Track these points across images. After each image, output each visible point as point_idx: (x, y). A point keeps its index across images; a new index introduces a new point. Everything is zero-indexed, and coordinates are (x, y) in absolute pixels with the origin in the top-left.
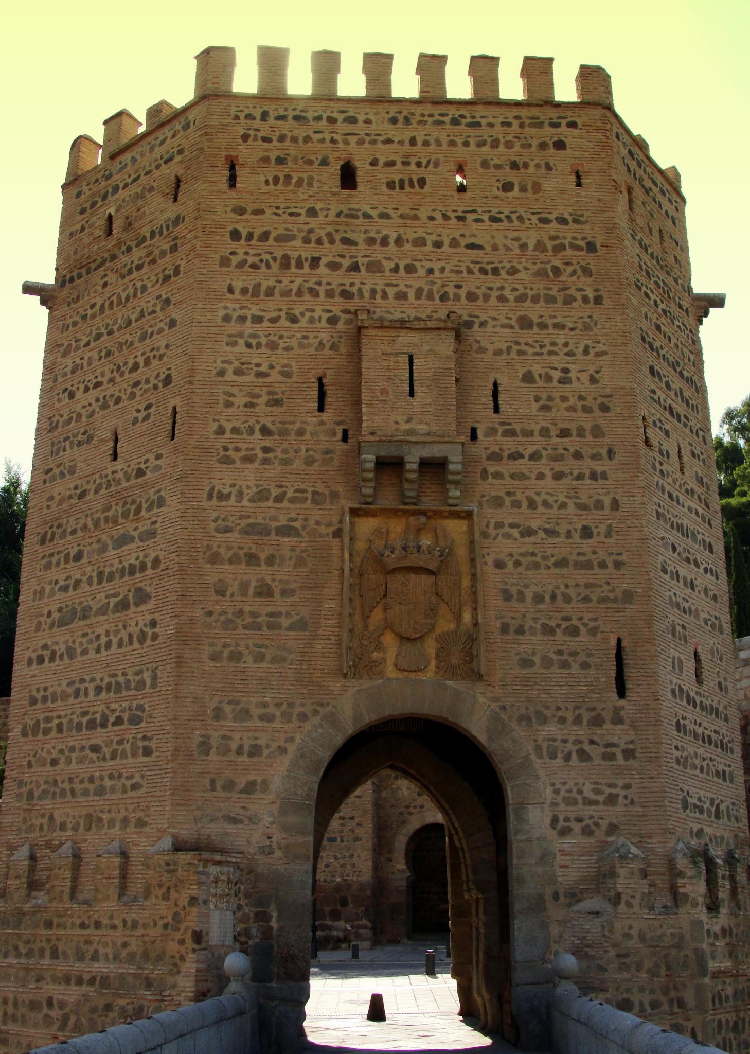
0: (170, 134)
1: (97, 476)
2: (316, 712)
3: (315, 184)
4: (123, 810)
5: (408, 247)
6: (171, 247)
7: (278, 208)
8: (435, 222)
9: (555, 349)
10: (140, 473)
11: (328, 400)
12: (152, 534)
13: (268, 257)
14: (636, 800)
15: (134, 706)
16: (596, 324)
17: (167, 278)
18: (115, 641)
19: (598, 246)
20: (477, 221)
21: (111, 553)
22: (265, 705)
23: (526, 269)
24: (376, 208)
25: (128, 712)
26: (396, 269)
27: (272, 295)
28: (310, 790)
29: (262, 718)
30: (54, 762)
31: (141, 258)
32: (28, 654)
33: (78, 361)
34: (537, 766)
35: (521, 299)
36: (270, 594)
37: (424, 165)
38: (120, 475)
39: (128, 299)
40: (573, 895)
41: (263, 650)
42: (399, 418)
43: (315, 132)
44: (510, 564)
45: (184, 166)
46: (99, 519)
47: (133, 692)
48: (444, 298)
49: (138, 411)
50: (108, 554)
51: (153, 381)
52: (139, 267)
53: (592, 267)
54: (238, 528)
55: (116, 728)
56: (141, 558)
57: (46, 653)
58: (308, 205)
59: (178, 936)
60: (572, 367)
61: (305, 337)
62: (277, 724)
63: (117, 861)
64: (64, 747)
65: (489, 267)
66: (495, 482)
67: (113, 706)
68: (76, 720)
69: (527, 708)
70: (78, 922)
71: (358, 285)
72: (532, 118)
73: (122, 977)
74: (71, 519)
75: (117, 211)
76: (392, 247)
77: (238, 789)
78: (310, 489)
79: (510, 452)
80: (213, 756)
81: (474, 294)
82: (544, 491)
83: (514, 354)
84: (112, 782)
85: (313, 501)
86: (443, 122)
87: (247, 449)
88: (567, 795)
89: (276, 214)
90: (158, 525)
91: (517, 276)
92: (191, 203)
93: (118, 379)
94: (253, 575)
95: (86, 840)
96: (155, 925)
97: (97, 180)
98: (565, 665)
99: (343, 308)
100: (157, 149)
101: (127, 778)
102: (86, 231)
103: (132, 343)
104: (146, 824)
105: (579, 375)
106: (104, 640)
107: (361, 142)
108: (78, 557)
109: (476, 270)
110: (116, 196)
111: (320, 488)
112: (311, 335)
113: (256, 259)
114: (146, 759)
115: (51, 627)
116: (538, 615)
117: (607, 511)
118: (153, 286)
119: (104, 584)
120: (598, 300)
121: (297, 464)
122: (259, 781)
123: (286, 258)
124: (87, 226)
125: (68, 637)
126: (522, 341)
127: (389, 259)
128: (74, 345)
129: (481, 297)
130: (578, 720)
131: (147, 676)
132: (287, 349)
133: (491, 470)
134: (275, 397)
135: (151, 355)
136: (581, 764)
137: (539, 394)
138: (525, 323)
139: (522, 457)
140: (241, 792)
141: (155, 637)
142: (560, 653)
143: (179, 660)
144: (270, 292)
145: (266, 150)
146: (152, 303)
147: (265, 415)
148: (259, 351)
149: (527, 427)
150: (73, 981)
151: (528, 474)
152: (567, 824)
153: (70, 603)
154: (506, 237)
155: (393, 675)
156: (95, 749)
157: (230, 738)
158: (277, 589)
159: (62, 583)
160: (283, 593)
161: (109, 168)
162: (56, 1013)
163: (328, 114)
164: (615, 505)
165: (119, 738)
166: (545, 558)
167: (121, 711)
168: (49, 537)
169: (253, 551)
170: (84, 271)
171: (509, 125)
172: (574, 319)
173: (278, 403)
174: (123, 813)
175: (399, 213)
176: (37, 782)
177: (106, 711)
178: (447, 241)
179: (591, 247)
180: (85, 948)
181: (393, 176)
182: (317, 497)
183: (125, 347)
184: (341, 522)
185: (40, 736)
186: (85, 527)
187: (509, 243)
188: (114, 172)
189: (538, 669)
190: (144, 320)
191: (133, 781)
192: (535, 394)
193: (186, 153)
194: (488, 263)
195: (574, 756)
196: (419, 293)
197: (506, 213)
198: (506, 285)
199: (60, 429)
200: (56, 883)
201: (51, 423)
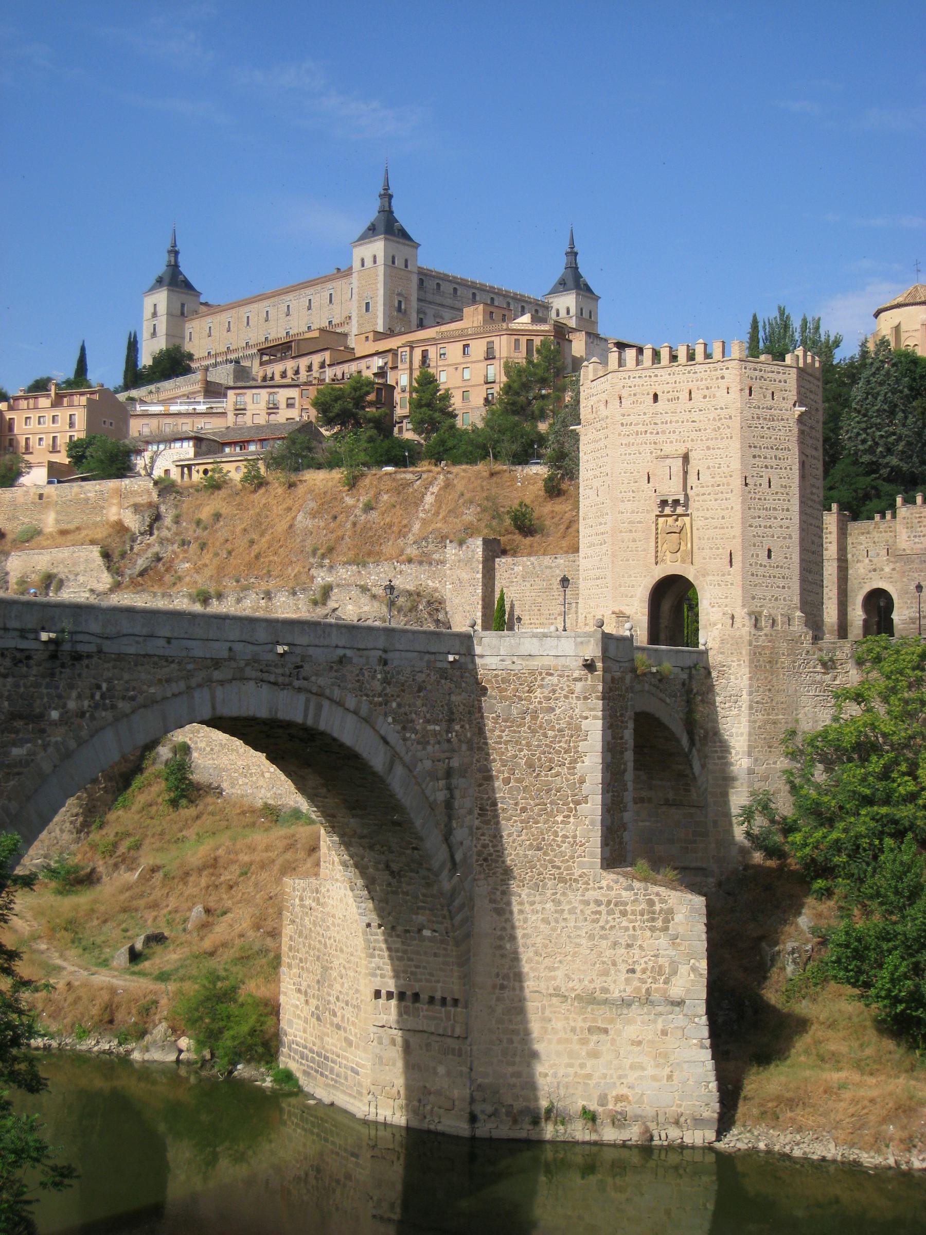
121: (642, 501)
138: (708, 448)
147: (634, 486)
164: (732, 508)
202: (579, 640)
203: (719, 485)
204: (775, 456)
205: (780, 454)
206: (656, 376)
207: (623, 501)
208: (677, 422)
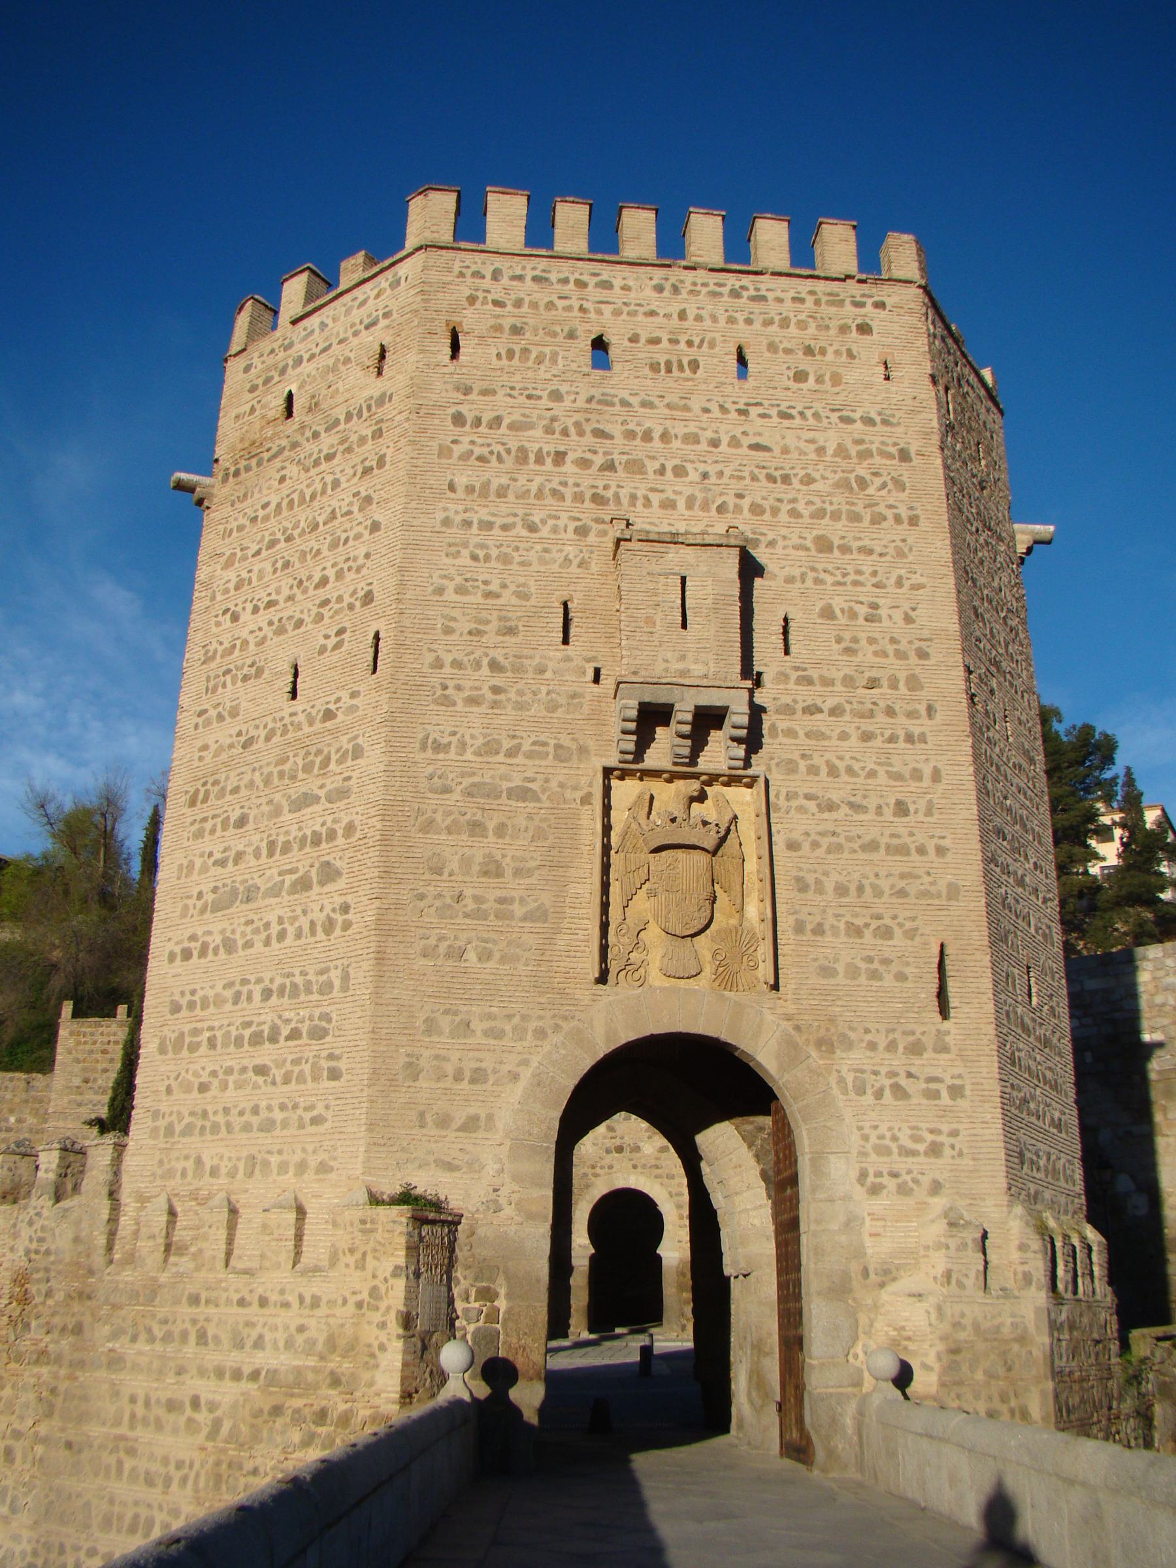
0: (373, 294)
1: (269, 719)
2: (557, 1028)
3: (560, 361)
4: (299, 1151)
5: (676, 444)
6: (374, 433)
7: (512, 388)
8: (711, 415)
9: (861, 578)
10: (329, 715)
11: (573, 631)
12: (342, 794)
13: (500, 448)
14: (965, 1151)
15: (317, 1015)
16: (911, 549)
17: (367, 471)
18: (291, 930)
19: (913, 455)
20: (763, 416)
21: (287, 817)
22: (490, 1017)
23: (823, 478)
24: (636, 394)
25: (307, 1022)
26: (662, 471)
27: (505, 496)
28: (549, 1128)
29: (487, 1033)
30: (203, 1088)
31: (332, 446)
32: (170, 946)
33: (245, 575)
34: (841, 1104)
35: (819, 514)
36: (499, 873)
37: (696, 344)
38: (301, 718)
39: (313, 497)
40: (887, 1272)
41: (490, 945)
42: (669, 655)
43: (560, 298)
44: (806, 846)
45: (391, 332)
46: (270, 774)
47: (316, 997)
48: (721, 509)
49: (327, 637)
50: (282, 819)
51: (347, 599)
52: (330, 457)
53: (904, 479)
54: (459, 788)
55: (290, 1043)
56: (329, 824)
57: (195, 946)
58: (551, 388)
59: (377, 1317)
60: (881, 602)
61: (546, 551)
62: (506, 1042)
63: (292, 1216)
64: (217, 1068)
65: (777, 474)
66: (785, 740)
67: (287, 1015)
68: (234, 1033)
69: (828, 1030)
70: (236, 1297)
71: (613, 489)
72: (830, 294)
73: (298, 1371)
74: (232, 774)
75: (300, 388)
76: (657, 443)
77: (455, 1125)
78: (552, 742)
79: (806, 704)
80: (423, 1083)
81: (760, 506)
82: (847, 756)
83: (809, 583)
84: (284, 1114)
85: (557, 757)
86: (720, 294)
87: (471, 688)
88: (878, 1142)
89: (510, 395)
90: (351, 782)
91: (813, 487)
92: (400, 377)
93: (299, 596)
94: (479, 849)
95: (246, 1191)
96: (345, 1301)
97: (272, 351)
98: (874, 975)
99: (594, 516)
100: (355, 311)
101: (306, 1109)
102: (257, 413)
103: (319, 552)
104: (332, 1169)
105: (890, 612)
106: (275, 929)
107: (617, 313)
108: (242, 822)
109: (762, 477)
110: (299, 370)
111: (565, 741)
112: (554, 548)
113: (485, 451)
114: (333, 1084)
115: (203, 911)
116: (842, 911)
117: (926, 782)
118: (348, 481)
119: (277, 856)
120: (913, 521)
122: (483, 1116)
123: (522, 450)
124: (258, 407)
125: (225, 924)
126: (820, 566)
127: (653, 458)
128: (239, 554)
129: (768, 510)
130: (891, 1046)
131: (335, 976)
132: (522, 564)
133: (782, 725)
134: (508, 624)
135: (346, 567)
136: (896, 1103)
137: (841, 633)
138: (824, 545)
139: (820, 711)
140: (458, 1130)
141: (347, 926)
142: (870, 960)
143: (380, 956)
144: (502, 492)
145: (498, 317)
146: (347, 501)
147: (495, 645)
148: (487, 565)
149: (826, 674)
150: (227, 1375)
151: (828, 733)
152: (879, 1180)
153: (229, 881)
154: (799, 438)
155: (657, 984)
156: (261, 1070)
157: (446, 1059)
158: (508, 865)
159: (218, 856)
160: (517, 873)
161: (288, 335)
162: (203, 1417)
163: (577, 276)
164: (936, 776)
165: (294, 1056)
166: (849, 839)
167: (298, 1021)
168: (201, 796)
169: (478, 817)
170: (254, 462)
171: (802, 301)
172: (883, 543)
173: (511, 631)
174: (298, 1157)
175: (666, 401)
176: (179, 1113)
177: (279, 1022)
178: (725, 440)
179: (904, 456)
180: (245, 1332)
181: (657, 356)
182: (560, 752)
183: (309, 557)
184: (590, 785)
185: (185, 1053)
186: (251, 784)
187: (802, 445)
188: (296, 341)
189: (841, 979)
190: (336, 523)
191: (315, 1113)
192: (837, 633)
193: (395, 316)
194: (776, 469)
195: (887, 1093)
196: (690, 502)
197: (799, 408)
198: (800, 497)
199: (218, 660)
200: (204, 1245)
201: (207, 652)
203: (872, 684)
206: (607, 285)
207: (447, 701)
208: (693, 439)
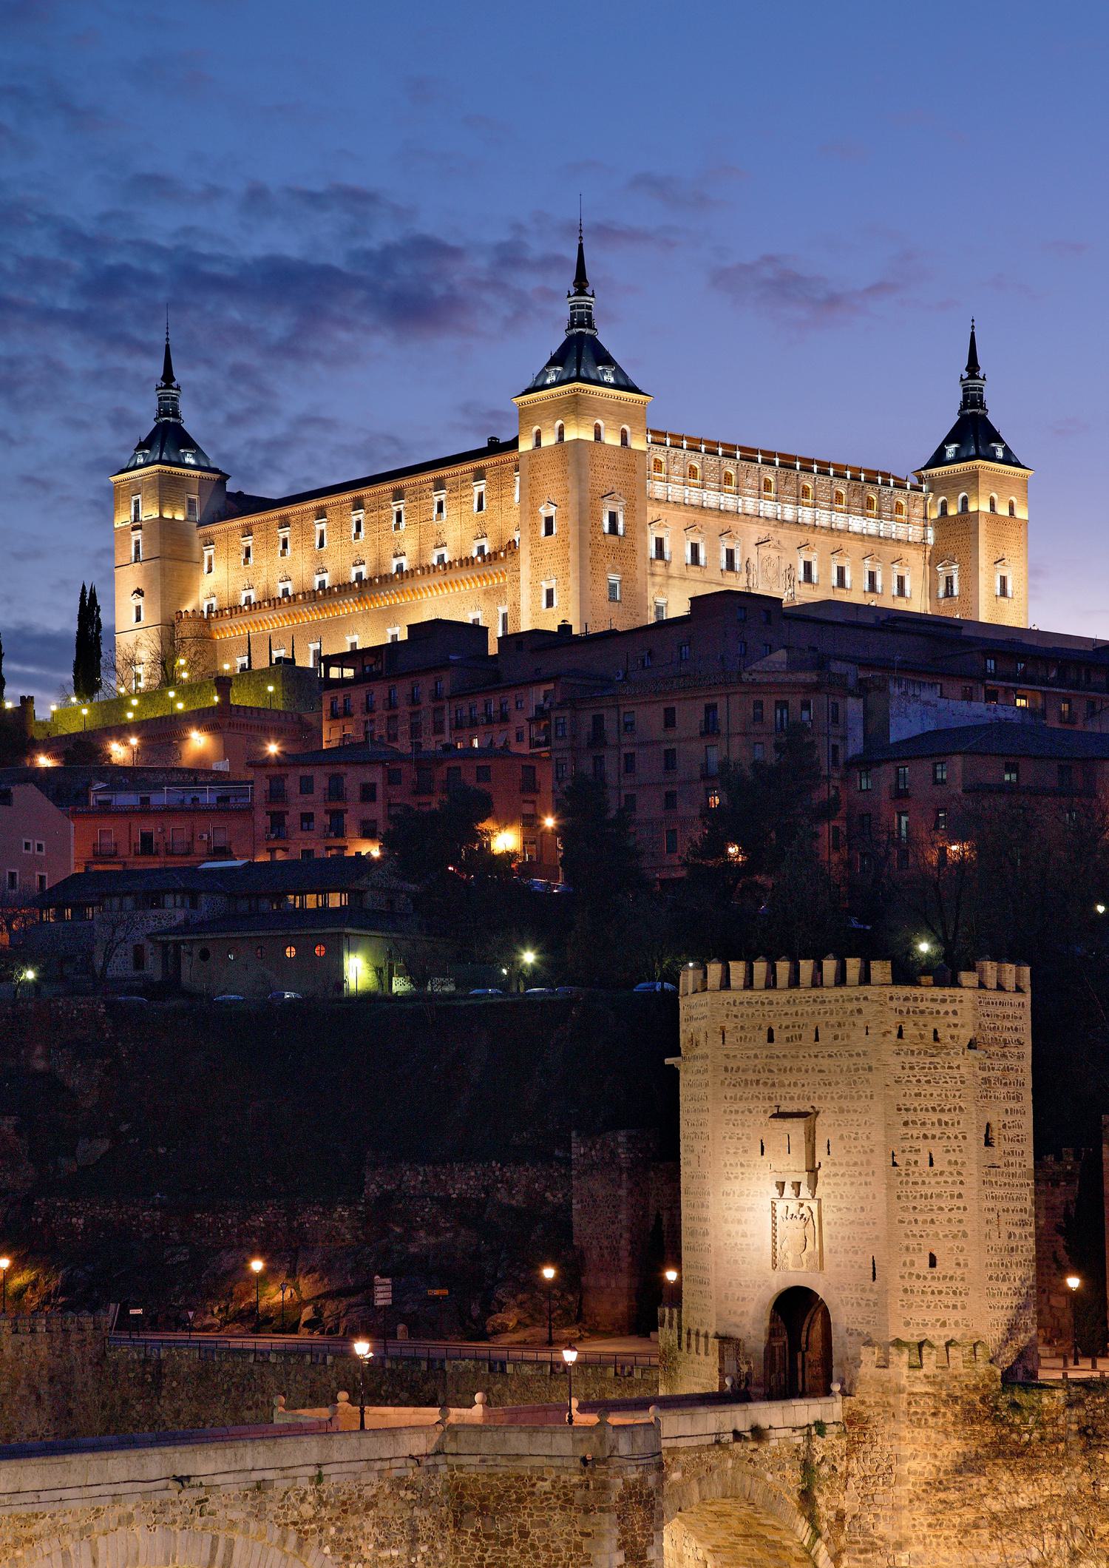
35: (840, 1097)
65: (827, 1082)
123: (746, 1080)
132: (748, 1126)
133: (826, 1182)
179: (870, 1069)
202: (578, 1436)
204: (940, 1121)
205: (945, 1117)
